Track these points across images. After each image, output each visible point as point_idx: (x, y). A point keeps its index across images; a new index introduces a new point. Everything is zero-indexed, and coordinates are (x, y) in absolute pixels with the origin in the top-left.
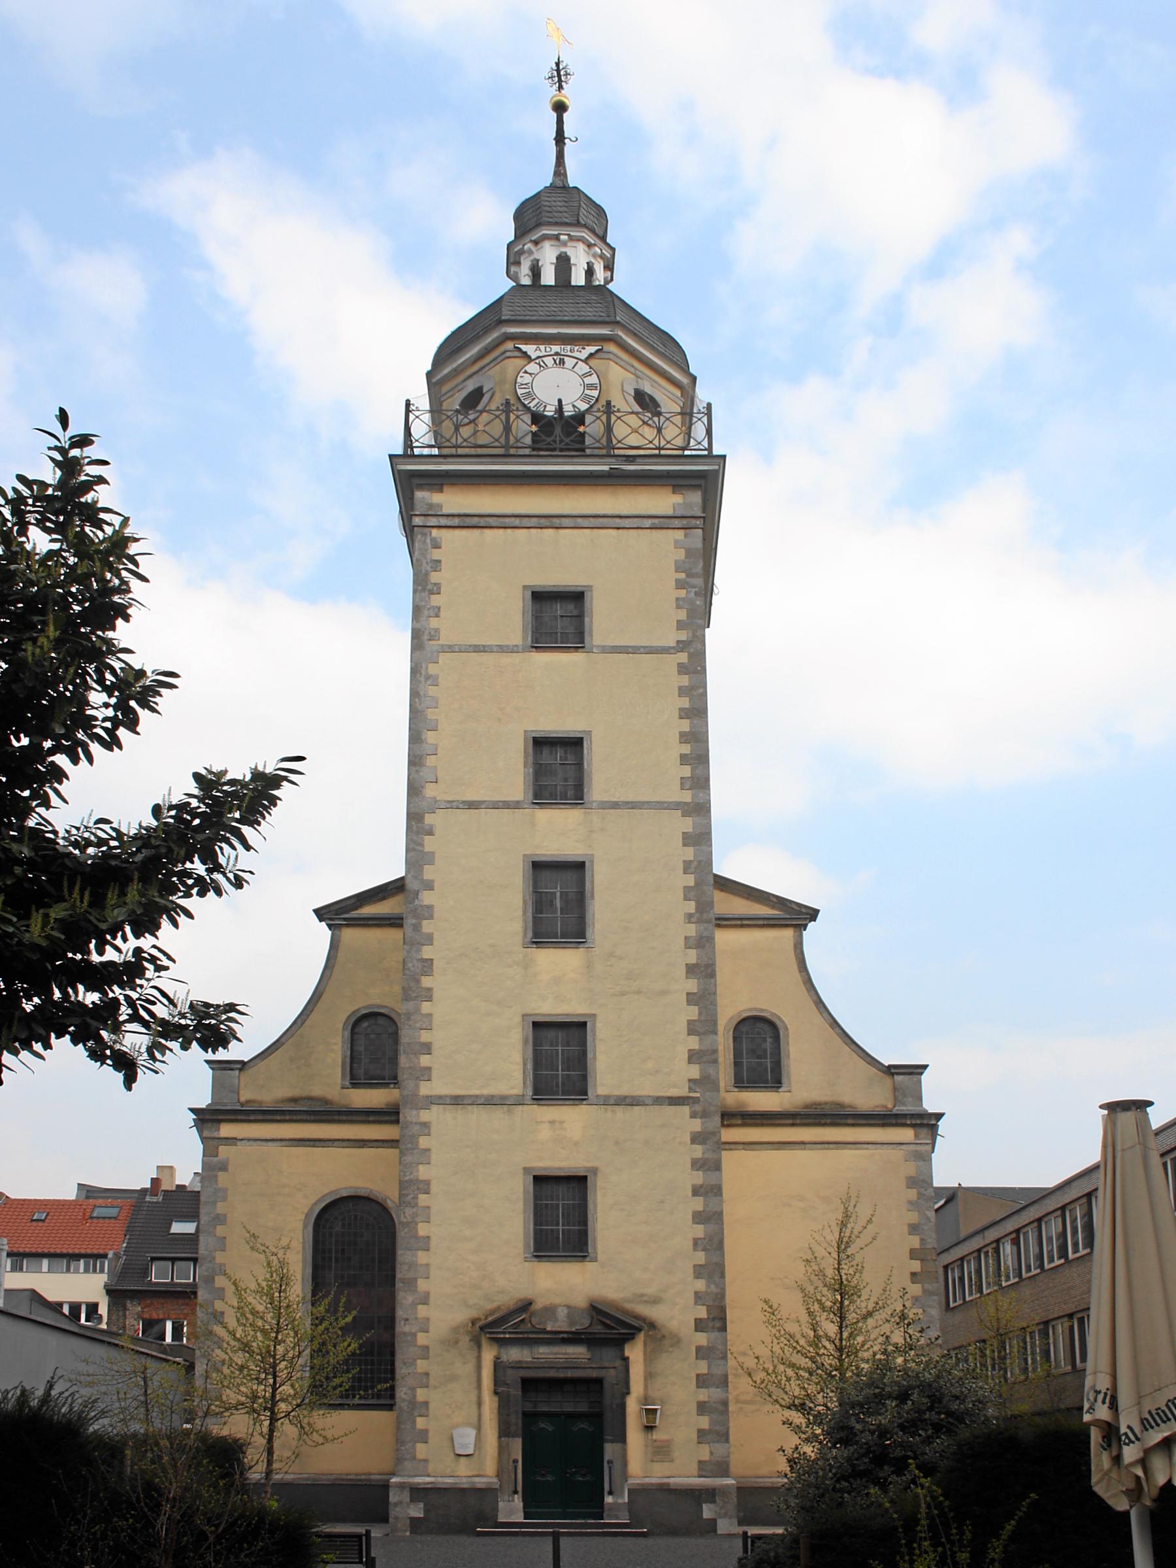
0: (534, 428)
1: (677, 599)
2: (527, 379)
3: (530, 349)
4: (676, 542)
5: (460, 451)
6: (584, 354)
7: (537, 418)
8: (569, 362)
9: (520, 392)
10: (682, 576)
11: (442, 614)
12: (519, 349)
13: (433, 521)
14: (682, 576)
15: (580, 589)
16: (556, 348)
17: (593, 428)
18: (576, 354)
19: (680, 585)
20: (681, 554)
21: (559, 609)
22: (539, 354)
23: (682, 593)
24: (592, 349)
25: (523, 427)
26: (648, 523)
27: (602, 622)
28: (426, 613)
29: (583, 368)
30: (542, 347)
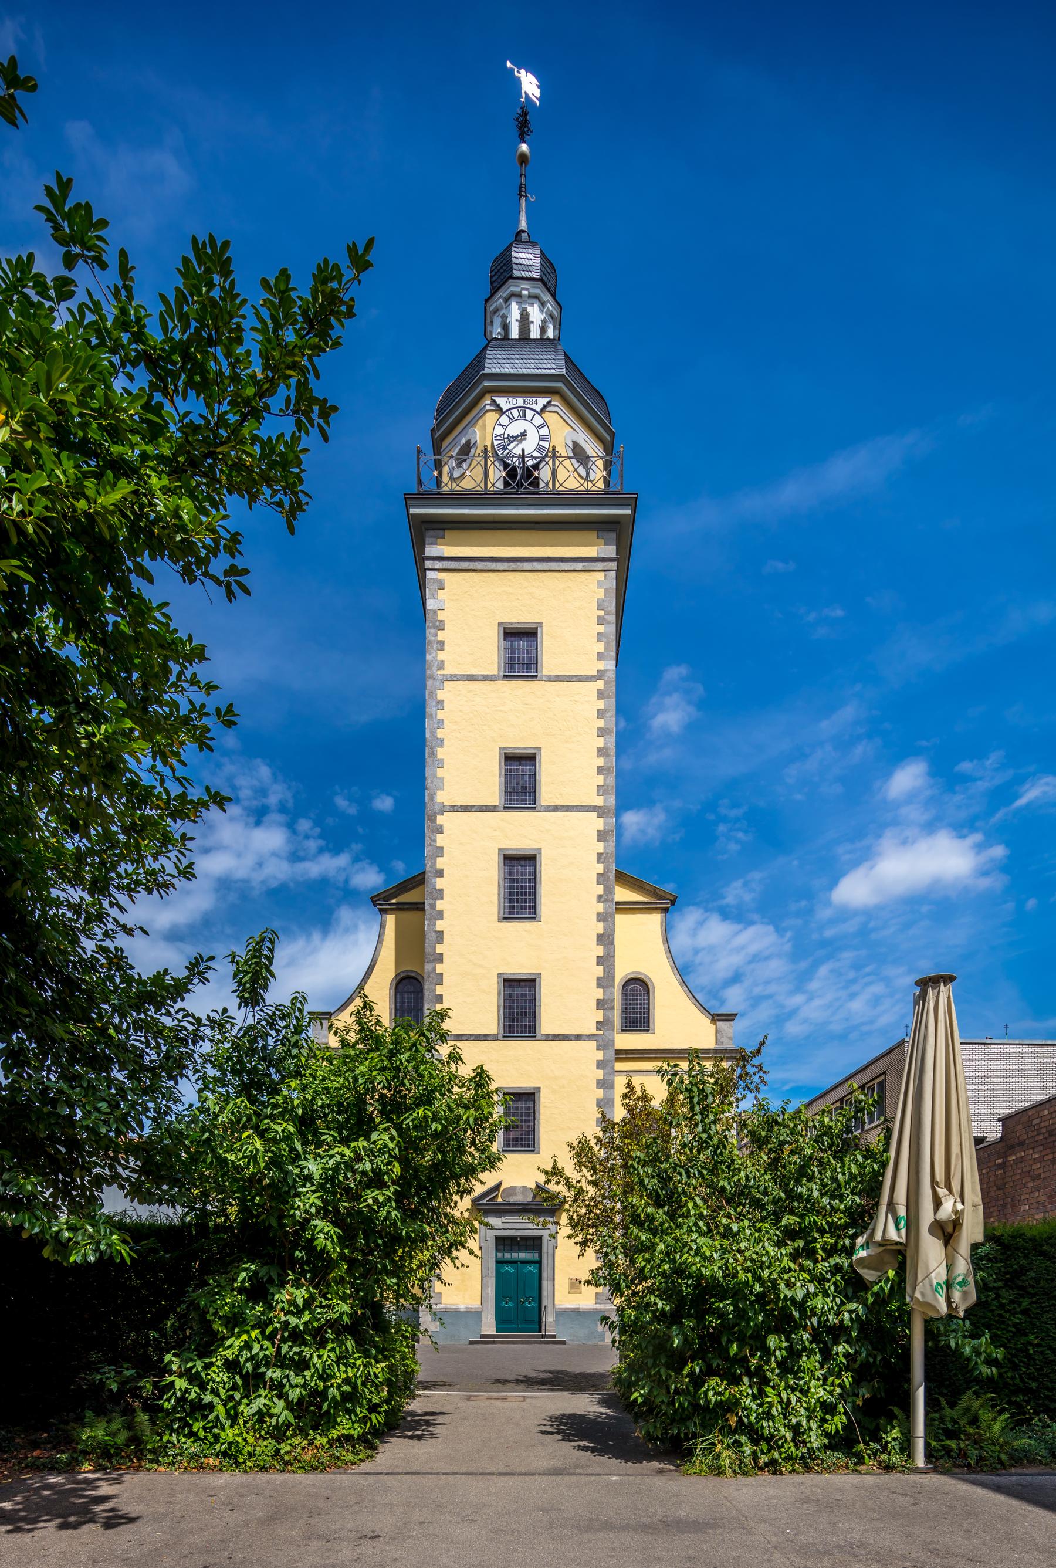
3: (501, 401)
4: (599, 582)
6: (538, 408)
8: (529, 414)
9: (496, 443)
10: (601, 613)
13: (438, 565)
14: (601, 613)
16: (520, 401)
18: (534, 406)
19: (601, 621)
20: (601, 594)
21: (523, 644)
23: (601, 629)
25: (496, 475)
26: (580, 566)
28: (435, 646)
29: (538, 420)
30: (511, 399)
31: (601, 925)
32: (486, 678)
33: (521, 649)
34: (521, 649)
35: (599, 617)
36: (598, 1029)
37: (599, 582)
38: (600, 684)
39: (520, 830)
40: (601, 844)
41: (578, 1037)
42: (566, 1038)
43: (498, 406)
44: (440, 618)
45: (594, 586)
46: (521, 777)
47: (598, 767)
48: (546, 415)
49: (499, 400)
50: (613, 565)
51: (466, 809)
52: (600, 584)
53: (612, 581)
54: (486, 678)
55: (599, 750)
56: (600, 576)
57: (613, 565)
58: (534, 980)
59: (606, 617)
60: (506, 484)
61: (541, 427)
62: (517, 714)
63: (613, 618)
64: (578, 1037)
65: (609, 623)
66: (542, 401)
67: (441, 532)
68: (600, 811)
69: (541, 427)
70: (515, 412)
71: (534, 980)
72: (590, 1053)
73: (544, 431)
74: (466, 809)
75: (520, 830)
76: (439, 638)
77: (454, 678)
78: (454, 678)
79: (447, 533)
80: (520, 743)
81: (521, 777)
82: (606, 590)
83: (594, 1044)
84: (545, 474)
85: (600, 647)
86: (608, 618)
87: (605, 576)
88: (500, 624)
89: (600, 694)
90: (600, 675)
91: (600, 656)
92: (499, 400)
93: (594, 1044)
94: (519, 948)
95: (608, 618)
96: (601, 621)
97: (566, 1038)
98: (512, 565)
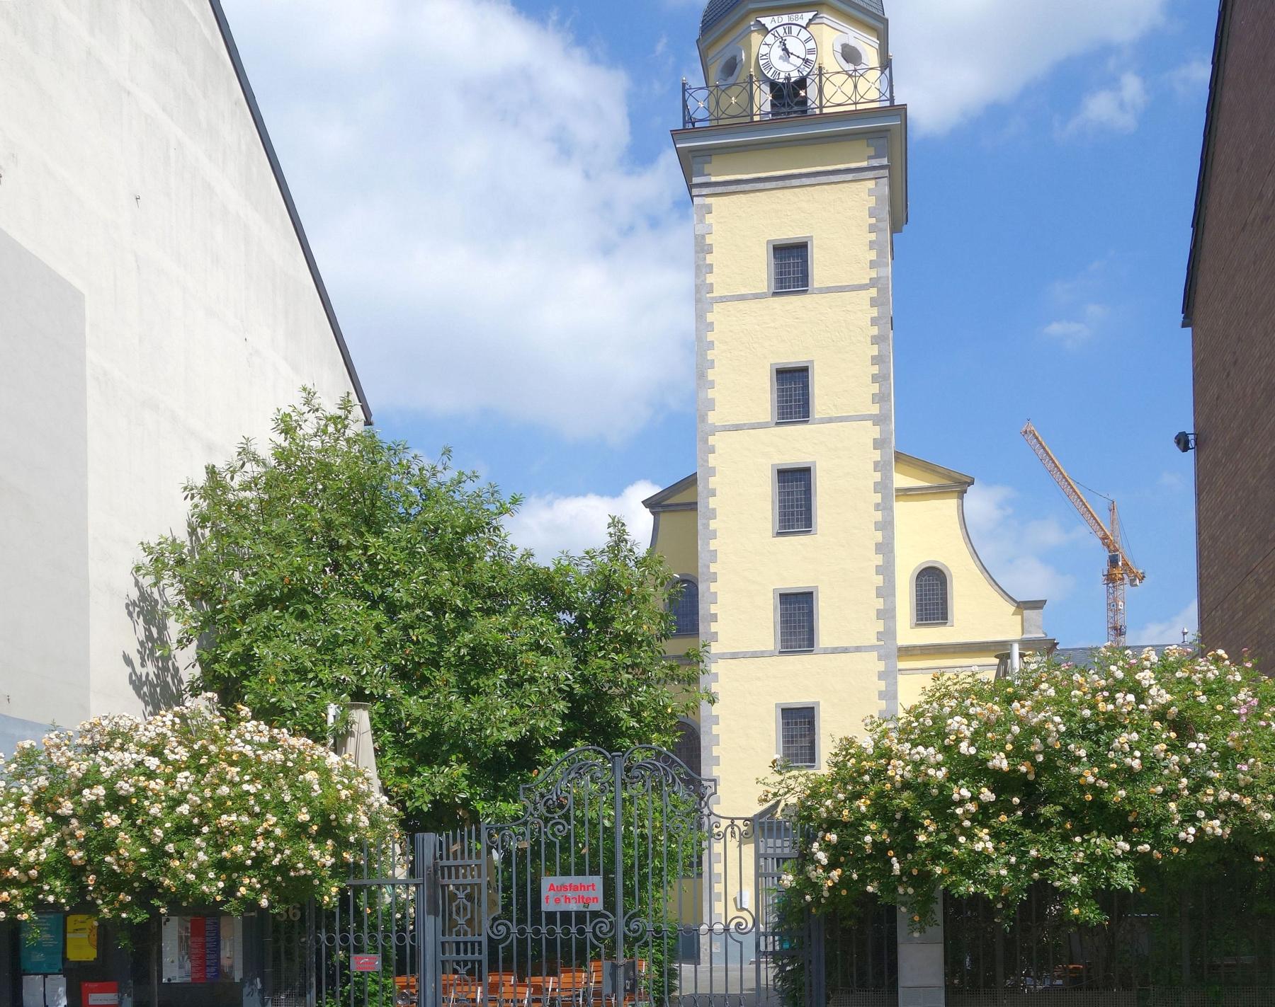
2: (764, 50)
3: (768, 21)
5: (721, 122)
7: (774, 86)
8: (795, 29)
9: (761, 62)
10: (873, 221)
13: (705, 191)
14: (873, 221)
16: (785, 19)
18: (799, 22)
22: (774, 25)
25: (763, 99)
26: (850, 177)
27: (820, 271)
29: (804, 35)
31: (879, 534)
32: (757, 296)
33: (791, 265)
34: (791, 265)
36: (878, 639)
38: (873, 292)
39: (795, 444)
40: (878, 452)
41: (858, 649)
42: (845, 650)
45: (865, 195)
46: (793, 391)
47: (873, 376)
48: (812, 28)
50: (886, 172)
51: (737, 428)
54: (757, 296)
55: (873, 358)
56: (871, 184)
58: (811, 593)
60: (773, 105)
61: (807, 41)
62: (793, 329)
64: (858, 649)
66: (808, 16)
67: (708, 158)
68: (878, 420)
69: (807, 41)
70: (781, 30)
71: (811, 593)
72: (871, 664)
73: (811, 45)
74: (737, 428)
75: (795, 444)
76: (708, 262)
77: (723, 299)
78: (723, 299)
80: (791, 359)
81: (793, 391)
83: (875, 654)
84: (811, 92)
85: (873, 255)
86: (881, 225)
88: (768, 242)
89: (874, 303)
90: (873, 283)
91: (873, 264)
92: (763, 20)
93: (875, 654)
94: (794, 564)
95: (881, 225)
96: (872, 229)
97: (845, 650)
98: (780, 184)
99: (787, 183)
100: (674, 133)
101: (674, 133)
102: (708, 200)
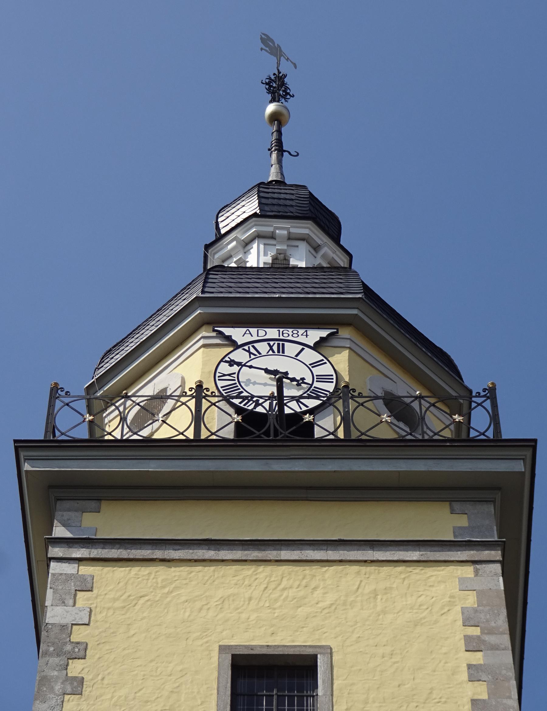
0: (239, 418)
1: (470, 666)
4: (462, 580)
8: (291, 349)
9: (220, 384)
10: (475, 631)
11: (86, 691)
12: (220, 333)
14: (475, 631)
15: (310, 651)
16: (273, 333)
17: (327, 425)
19: (472, 645)
23: (478, 658)
24: (324, 333)
28: (58, 687)
30: (253, 331)
35: (468, 639)
37: (462, 580)
43: (229, 338)
44: (75, 638)
45: (453, 587)
49: (227, 331)
50: (497, 554)
52: (464, 586)
53: (493, 579)
56: (468, 571)
57: (497, 554)
59: (486, 638)
61: (315, 364)
63: (506, 640)
65: (495, 648)
66: (315, 335)
67: (93, 504)
79: (104, 504)
82: (481, 594)
86: (492, 639)
87: (476, 572)
88: (223, 649)
92: (227, 331)
95: (492, 639)
99: (272, 554)
100: (20, 446)
101: (20, 446)
102: (86, 570)
